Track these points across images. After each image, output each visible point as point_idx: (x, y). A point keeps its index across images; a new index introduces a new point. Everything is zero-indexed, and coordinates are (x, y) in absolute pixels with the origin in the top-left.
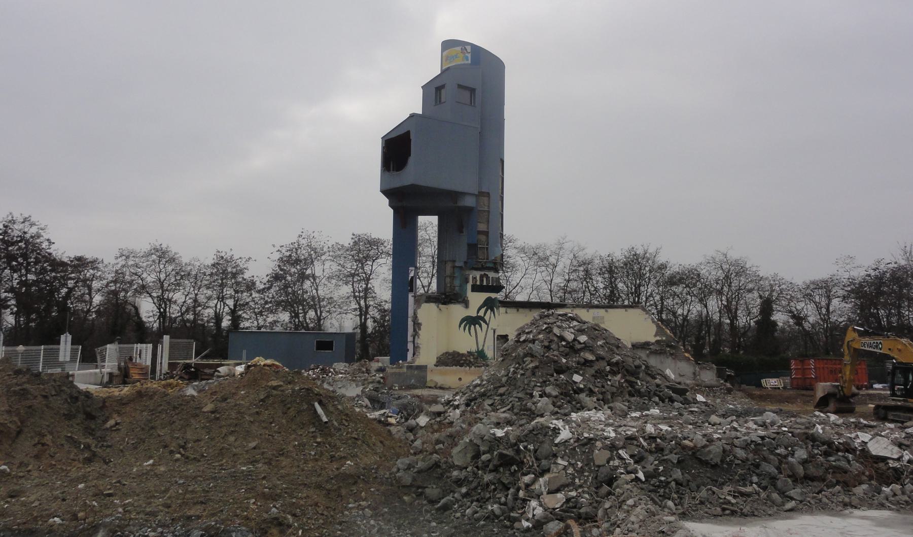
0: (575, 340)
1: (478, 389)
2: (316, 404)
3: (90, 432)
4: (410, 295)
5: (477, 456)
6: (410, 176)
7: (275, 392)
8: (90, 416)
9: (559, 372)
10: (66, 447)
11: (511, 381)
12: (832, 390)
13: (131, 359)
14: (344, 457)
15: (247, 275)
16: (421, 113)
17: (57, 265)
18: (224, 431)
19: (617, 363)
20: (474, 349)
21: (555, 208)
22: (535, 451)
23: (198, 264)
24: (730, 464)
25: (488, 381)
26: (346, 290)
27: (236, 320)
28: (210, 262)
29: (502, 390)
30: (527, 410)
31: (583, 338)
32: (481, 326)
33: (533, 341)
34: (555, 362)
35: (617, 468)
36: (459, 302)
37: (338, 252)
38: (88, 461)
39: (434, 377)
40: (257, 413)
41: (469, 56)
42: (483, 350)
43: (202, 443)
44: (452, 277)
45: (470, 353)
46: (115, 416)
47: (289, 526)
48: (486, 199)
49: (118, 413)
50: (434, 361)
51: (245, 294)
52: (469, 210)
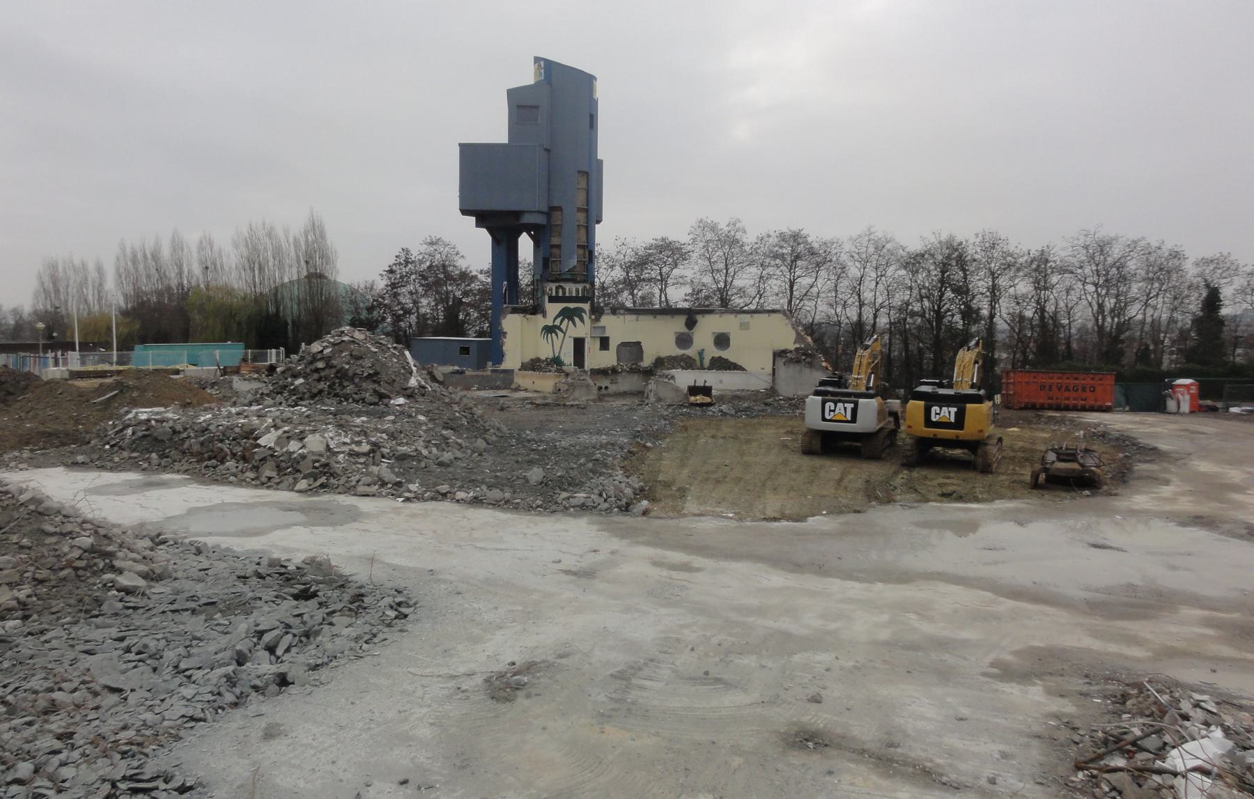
16: (504, 139)
20: (551, 356)
39: (519, 380)
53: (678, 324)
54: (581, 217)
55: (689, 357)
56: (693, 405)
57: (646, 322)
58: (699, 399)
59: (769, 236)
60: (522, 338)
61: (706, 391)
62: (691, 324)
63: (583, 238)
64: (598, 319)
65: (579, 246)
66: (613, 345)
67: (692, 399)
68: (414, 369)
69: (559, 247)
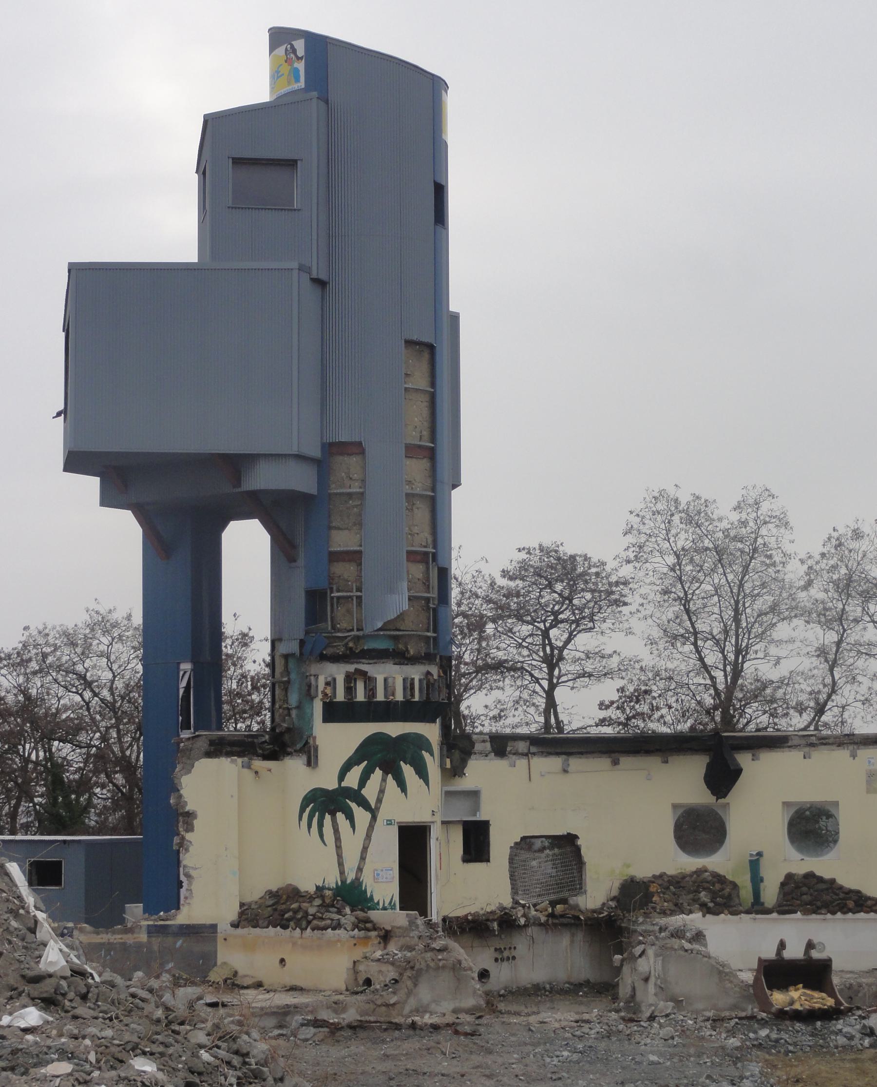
20: (332, 879)
32: (350, 817)
41: (301, 66)
42: (357, 883)
48: (354, 460)
50: (232, 912)
54: (417, 469)
55: (720, 879)
56: (783, 1016)
57: (591, 772)
58: (797, 997)
59: (857, 535)
60: (239, 830)
61: (814, 972)
63: (425, 535)
64: (456, 771)
65: (412, 556)
66: (500, 844)
67: (778, 998)
68: (41, 916)
69: (354, 557)
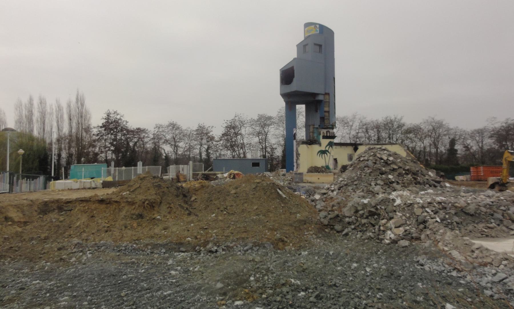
0: (388, 159)
1: (343, 182)
2: (278, 190)
3: (186, 202)
4: (295, 142)
5: (357, 211)
6: (294, 87)
7: (259, 185)
8: (185, 196)
9: (382, 173)
10: (180, 209)
11: (359, 179)
12: (497, 181)
13: (179, 172)
14: (296, 213)
15: (211, 134)
17: (128, 131)
18: (242, 202)
19: (408, 170)
20: (324, 165)
21: (359, 98)
22: (385, 209)
23: (189, 130)
24: (480, 214)
25: (348, 179)
26: (256, 139)
27: (208, 154)
28: (195, 128)
29: (355, 183)
30: (370, 191)
31: (391, 159)
33: (368, 160)
34: (380, 169)
35: (426, 216)
36: (317, 144)
37: (253, 123)
38: (189, 214)
40: (254, 194)
43: (234, 207)
44: (313, 132)
45: (323, 167)
46: (194, 195)
47: (286, 242)
49: (195, 194)
50: (306, 170)
51: (210, 142)
52: (320, 102)
53: (349, 150)
62: (356, 149)
